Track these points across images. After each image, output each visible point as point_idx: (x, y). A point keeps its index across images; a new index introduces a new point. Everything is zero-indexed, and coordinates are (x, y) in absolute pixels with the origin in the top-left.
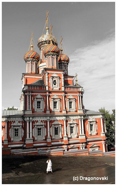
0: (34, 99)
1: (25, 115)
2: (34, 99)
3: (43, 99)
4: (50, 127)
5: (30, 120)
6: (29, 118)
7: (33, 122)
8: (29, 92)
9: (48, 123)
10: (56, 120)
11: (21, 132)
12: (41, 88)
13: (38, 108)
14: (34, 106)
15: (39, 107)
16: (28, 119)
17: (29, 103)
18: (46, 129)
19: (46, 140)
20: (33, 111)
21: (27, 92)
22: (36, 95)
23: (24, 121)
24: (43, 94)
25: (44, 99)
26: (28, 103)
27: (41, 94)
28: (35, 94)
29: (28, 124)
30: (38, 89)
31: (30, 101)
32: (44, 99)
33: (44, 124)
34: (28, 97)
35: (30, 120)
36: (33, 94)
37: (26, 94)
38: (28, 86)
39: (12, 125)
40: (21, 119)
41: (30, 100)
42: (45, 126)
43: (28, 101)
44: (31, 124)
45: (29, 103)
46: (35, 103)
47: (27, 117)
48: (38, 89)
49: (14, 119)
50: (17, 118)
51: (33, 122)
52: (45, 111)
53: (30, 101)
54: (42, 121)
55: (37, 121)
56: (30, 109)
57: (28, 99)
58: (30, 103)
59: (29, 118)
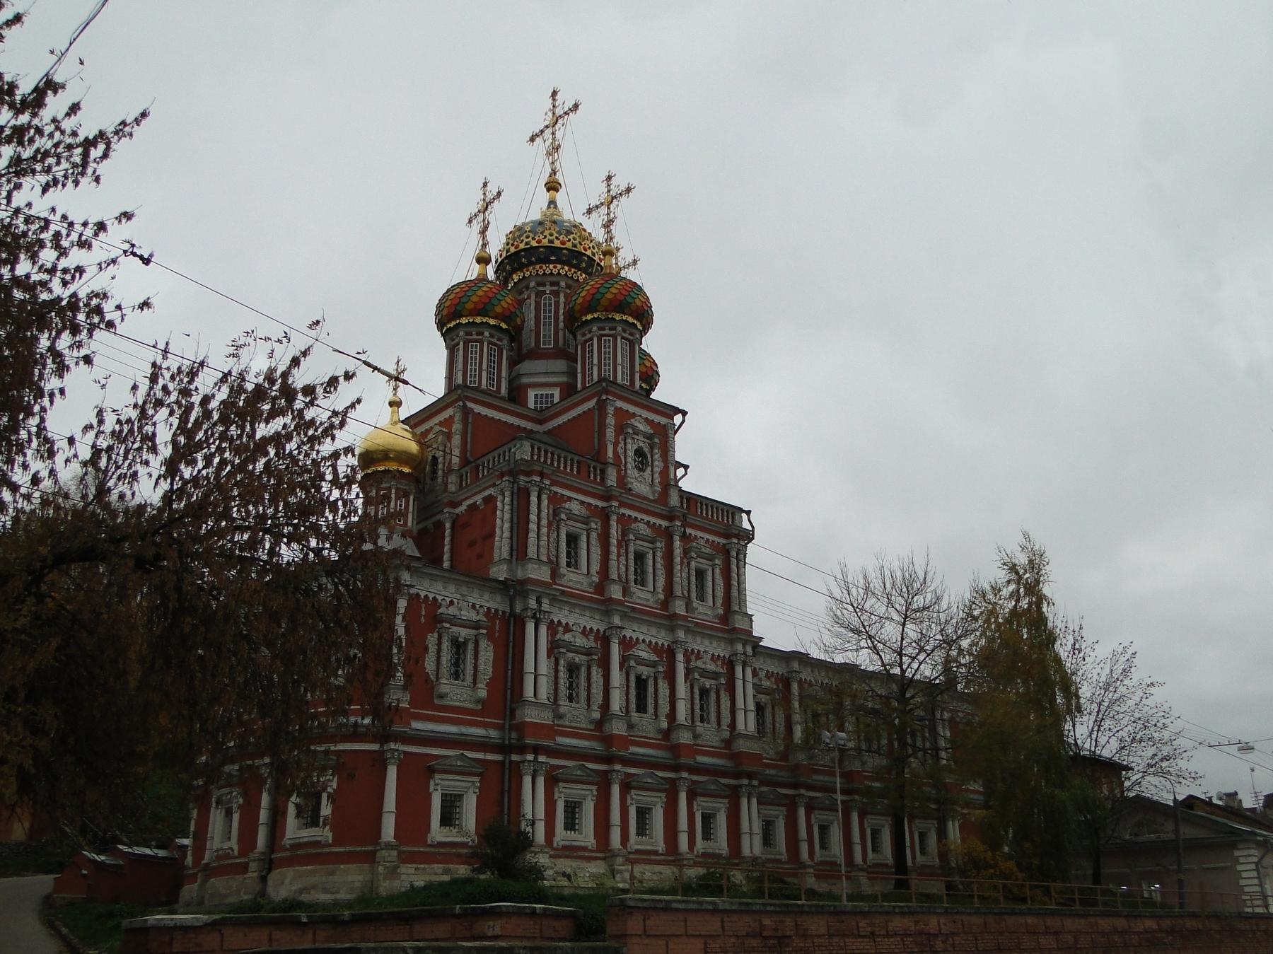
8: (542, 475)
10: (644, 641)
16: (532, 603)
19: (599, 724)
20: (555, 573)
21: (528, 474)
30: (572, 470)
31: (544, 522)
34: (534, 499)
38: (532, 447)
41: (544, 513)
43: (533, 517)
48: (572, 470)
51: (553, 627)
53: (544, 522)
54: (585, 633)
57: (534, 509)
58: (544, 530)
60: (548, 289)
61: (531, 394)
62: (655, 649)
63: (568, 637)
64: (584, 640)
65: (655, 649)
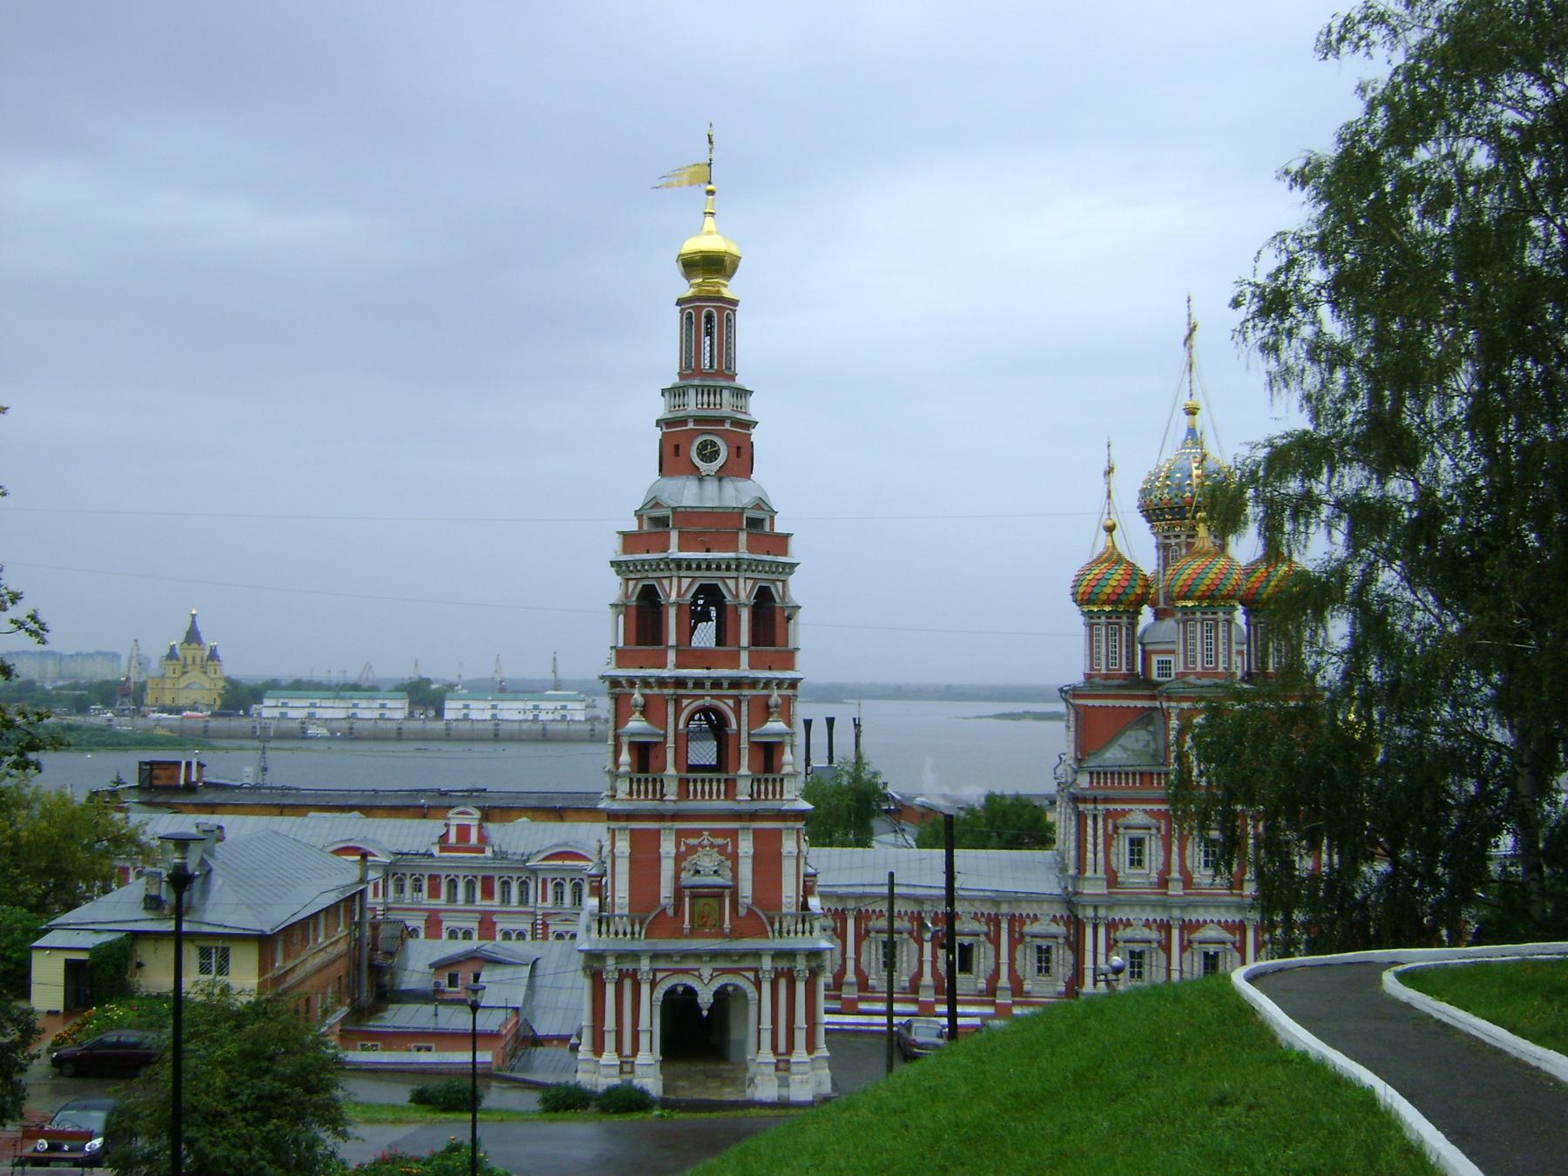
0: (1116, 828)
1: (1077, 893)
2: (1116, 828)
3: (1154, 831)
4: (1183, 949)
5: (1096, 917)
6: (1096, 908)
7: (1112, 926)
8: (1095, 800)
9: (1175, 934)
11: (1062, 959)
12: (1147, 780)
13: (1132, 863)
14: (1113, 858)
15: (1136, 861)
16: (1090, 912)
17: (1095, 846)
18: (1163, 956)
20: (1112, 880)
21: (1085, 800)
22: (1124, 813)
23: (1076, 916)
24: (1155, 807)
25: (1158, 829)
26: (1090, 847)
27: (1148, 807)
28: (1119, 807)
29: (1089, 932)
31: (1100, 840)
32: (1158, 829)
33: (1154, 935)
34: (1090, 822)
35: (1096, 917)
36: (1111, 807)
37: (1081, 807)
38: (1091, 773)
39: (1027, 929)
40: (1060, 911)
41: (1100, 832)
42: (1159, 942)
43: (1090, 839)
44: (1102, 931)
45: (1095, 846)
46: (1122, 847)
47: (1084, 907)
49: (1035, 906)
50: (1045, 906)
52: (1163, 882)
53: (1100, 840)
54: (1147, 924)
55: (1128, 924)
56: (1101, 873)
57: (1090, 831)
58: (1100, 847)
59: (1096, 908)
60: (1173, 541)
61: (1155, 659)
62: (1227, 926)
63: (1128, 933)
64: (1146, 931)
65: (1227, 926)
